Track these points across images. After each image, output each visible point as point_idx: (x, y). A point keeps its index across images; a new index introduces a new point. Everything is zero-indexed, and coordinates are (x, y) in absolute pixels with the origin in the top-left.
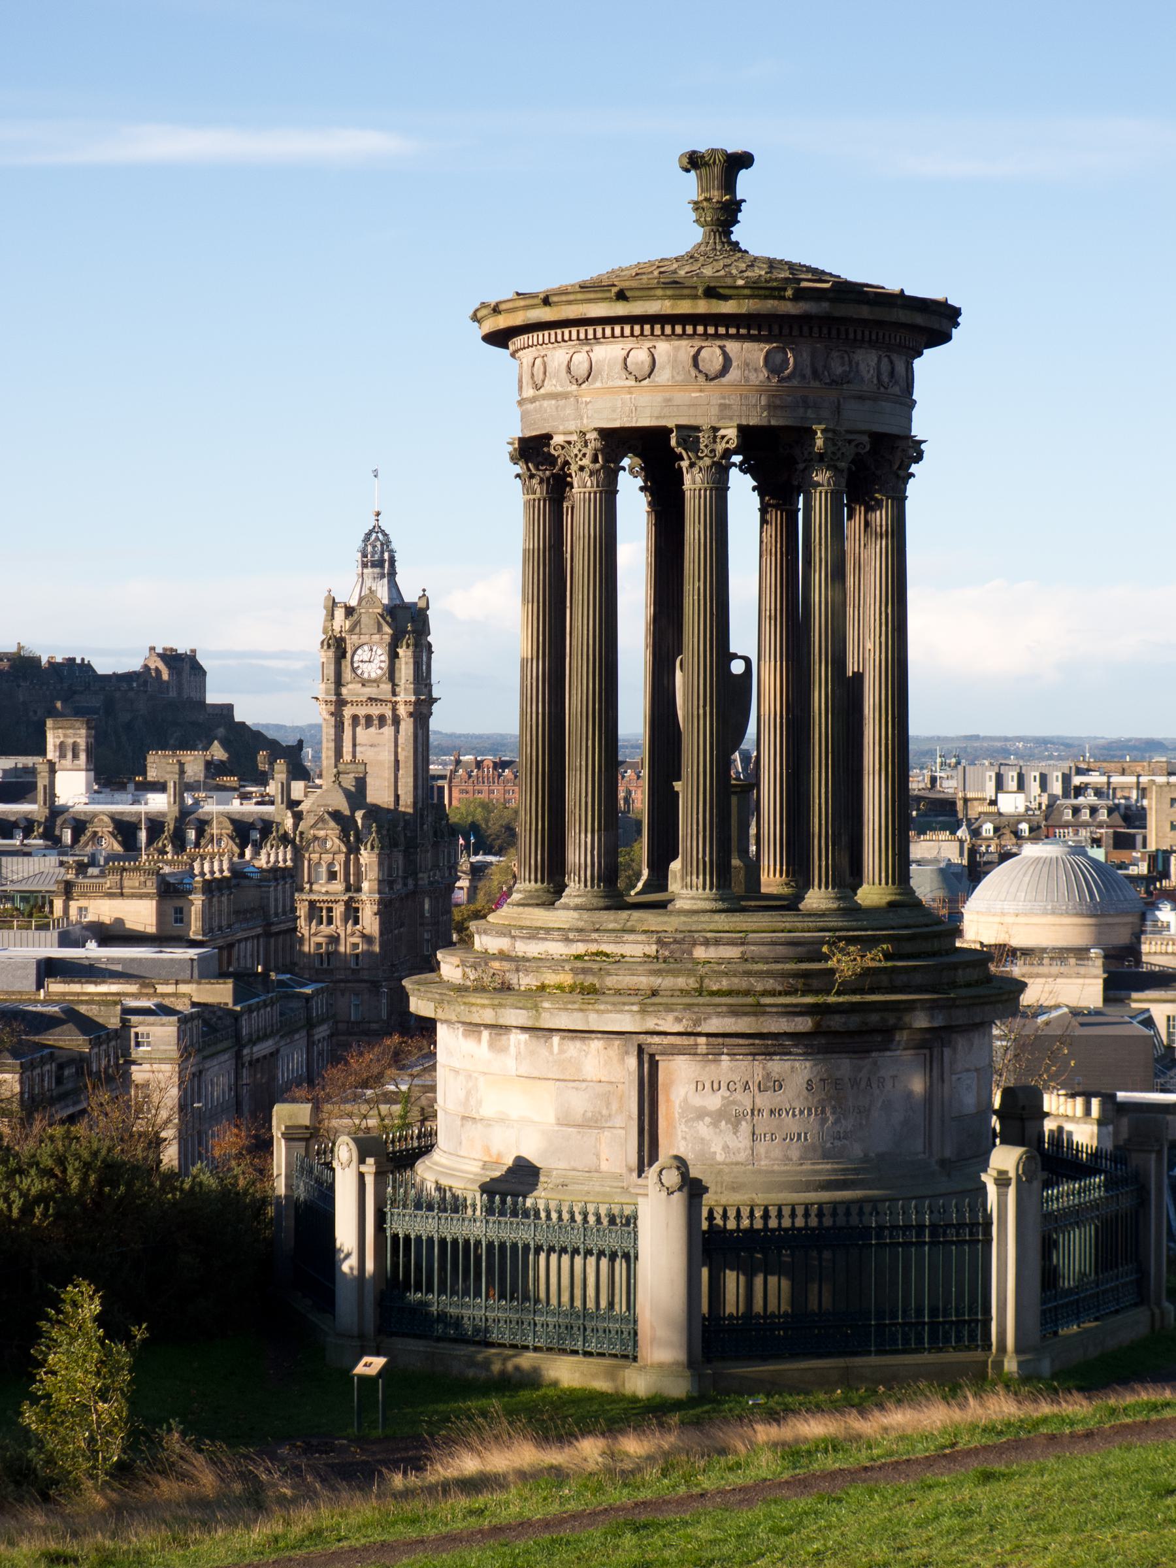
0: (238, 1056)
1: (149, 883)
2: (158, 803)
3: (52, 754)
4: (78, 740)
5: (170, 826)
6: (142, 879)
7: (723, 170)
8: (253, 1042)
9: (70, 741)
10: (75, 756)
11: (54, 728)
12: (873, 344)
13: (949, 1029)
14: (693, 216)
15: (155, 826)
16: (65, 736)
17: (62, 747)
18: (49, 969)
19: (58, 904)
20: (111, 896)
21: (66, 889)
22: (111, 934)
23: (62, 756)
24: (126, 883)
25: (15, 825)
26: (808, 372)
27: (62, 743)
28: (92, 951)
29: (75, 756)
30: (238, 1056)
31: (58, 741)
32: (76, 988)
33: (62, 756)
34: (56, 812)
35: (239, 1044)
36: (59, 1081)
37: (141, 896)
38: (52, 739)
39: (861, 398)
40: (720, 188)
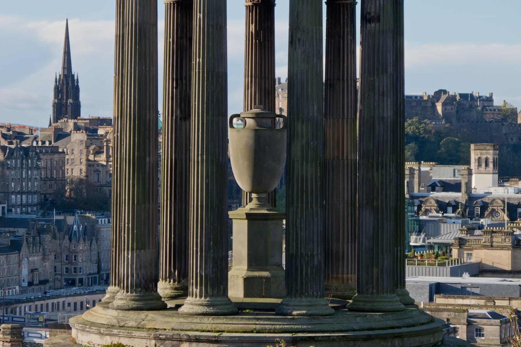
1: (507, 240)
3: (473, 165)
4: (489, 156)
6: (503, 237)
9: (484, 157)
10: (487, 165)
11: (475, 150)
16: (481, 154)
18: (438, 289)
19: (455, 252)
20: (485, 247)
21: (459, 242)
22: (480, 270)
23: (479, 165)
24: (495, 239)
25: (449, 204)
27: (479, 159)
28: (466, 279)
29: (487, 165)
31: (477, 157)
34: (471, 198)
37: (502, 248)
38: (474, 156)
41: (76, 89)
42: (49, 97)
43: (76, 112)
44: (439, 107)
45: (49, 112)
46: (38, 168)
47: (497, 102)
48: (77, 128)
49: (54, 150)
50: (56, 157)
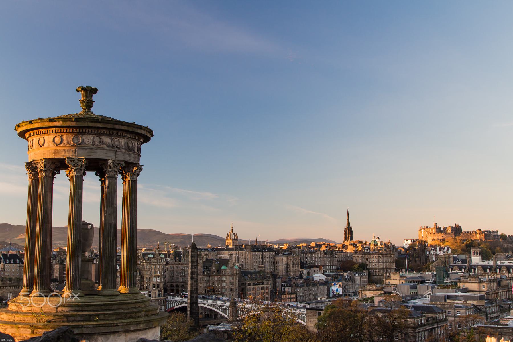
0: (487, 316)
2: (492, 263)
3: (472, 254)
5: (494, 268)
7: (89, 92)
8: (490, 313)
12: (89, 133)
13: (94, 334)
14: (81, 105)
15: (491, 268)
17: (474, 253)
18: (449, 297)
23: (474, 254)
26: (66, 143)
27: (474, 252)
28: (459, 293)
30: (487, 316)
32: (452, 302)
33: (474, 254)
35: (486, 314)
36: (427, 321)
38: (472, 251)
39: (84, 149)
40: (84, 97)
41: (351, 232)
42: (343, 234)
43: (352, 238)
44: (478, 236)
45: (343, 239)
46: (336, 257)
47: (499, 233)
48: (351, 244)
49: (342, 251)
50: (342, 254)
